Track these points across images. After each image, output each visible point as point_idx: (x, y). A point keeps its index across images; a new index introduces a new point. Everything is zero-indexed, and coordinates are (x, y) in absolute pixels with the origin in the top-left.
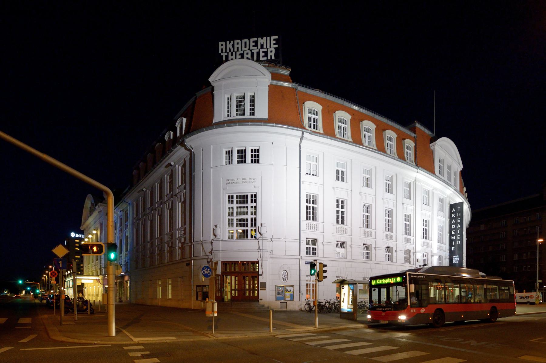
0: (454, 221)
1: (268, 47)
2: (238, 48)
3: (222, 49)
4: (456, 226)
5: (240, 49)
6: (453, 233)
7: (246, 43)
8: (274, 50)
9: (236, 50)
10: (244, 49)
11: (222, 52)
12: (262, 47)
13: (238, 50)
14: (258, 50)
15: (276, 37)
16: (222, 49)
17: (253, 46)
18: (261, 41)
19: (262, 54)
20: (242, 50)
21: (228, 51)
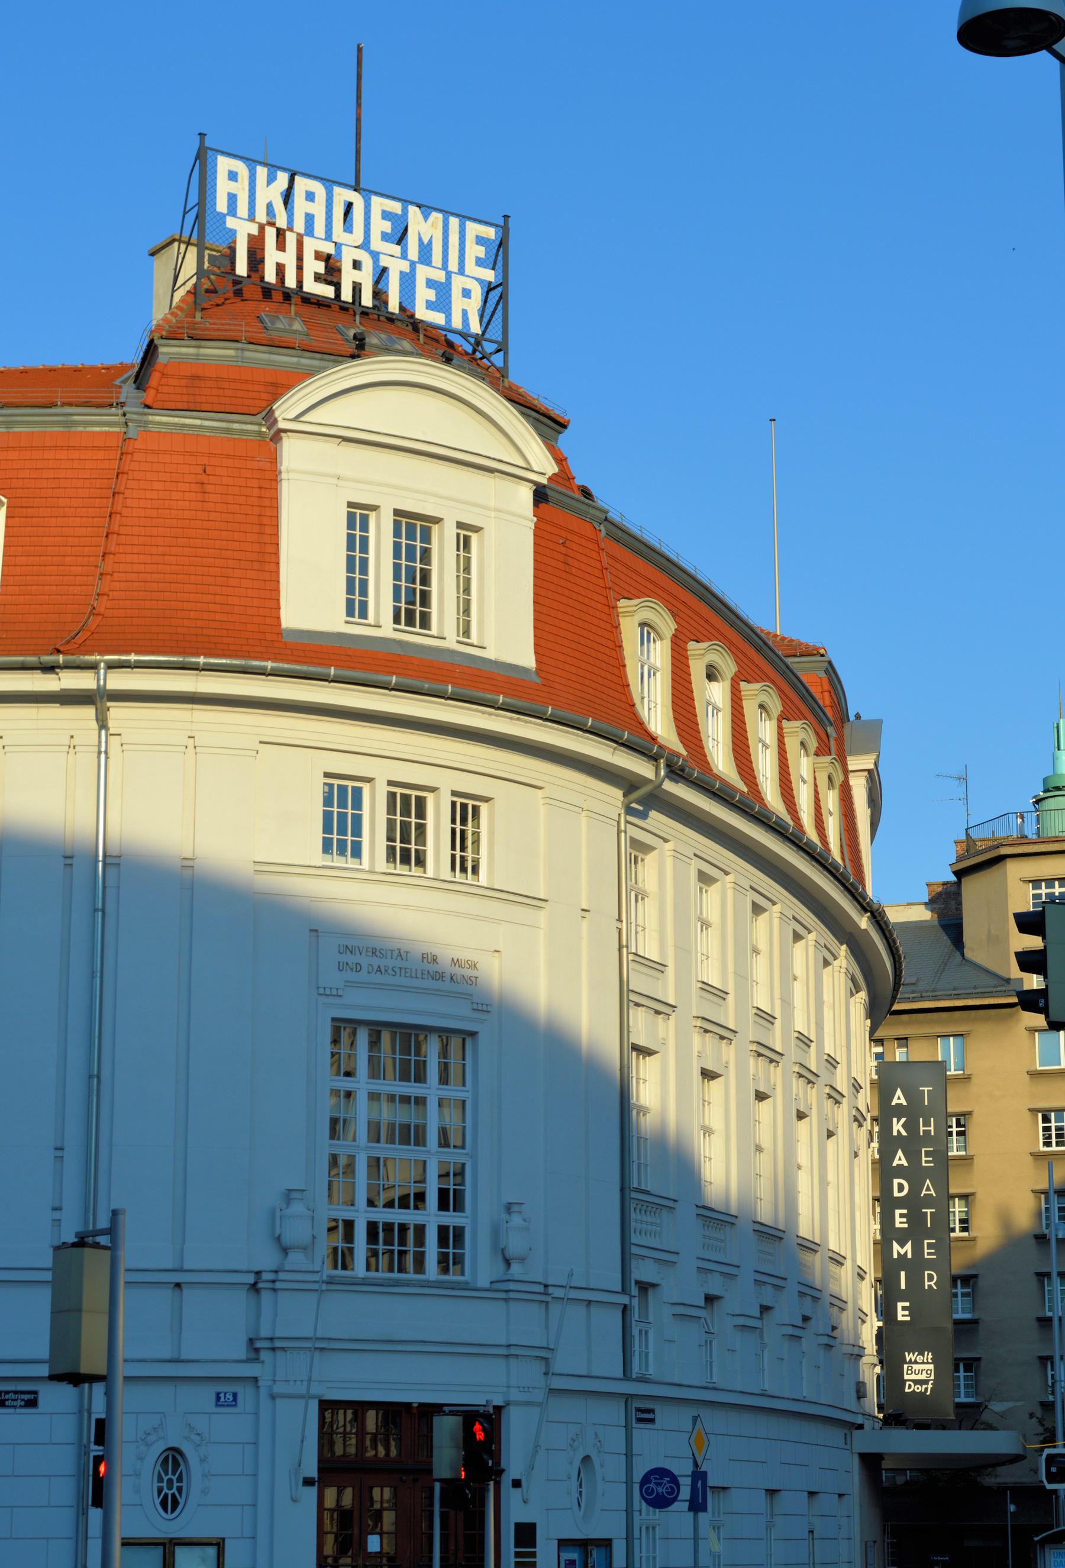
0: (900, 1159)
1: (453, 265)
2: (309, 219)
3: (232, 198)
4: (916, 1187)
5: (320, 228)
6: (900, 1222)
7: (349, 206)
8: (477, 293)
9: (299, 226)
12: (425, 250)
13: (310, 229)
14: (405, 266)
16: (232, 198)
17: (385, 237)
18: (423, 227)
19: (423, 294)
20: (328, 237)
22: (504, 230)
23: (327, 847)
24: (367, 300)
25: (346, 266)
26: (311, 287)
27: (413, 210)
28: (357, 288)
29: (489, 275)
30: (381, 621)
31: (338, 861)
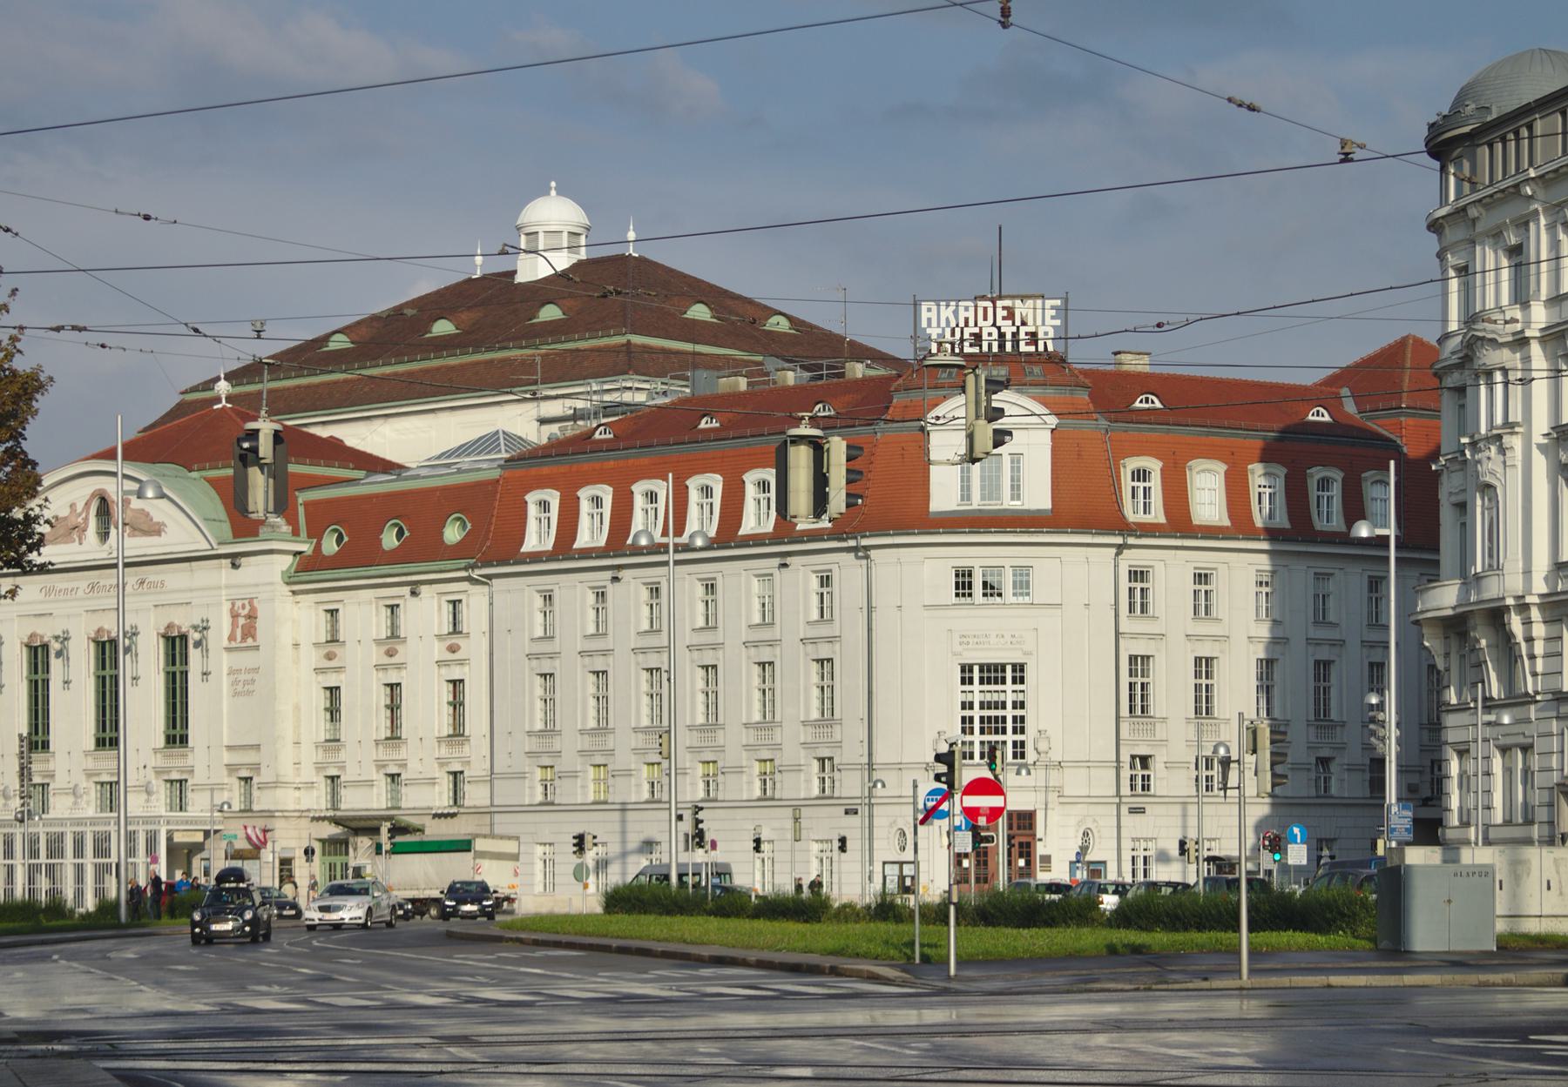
1: (1039, 322)
3: (929, 320)
5: (971, 323)
7: (985, 309)
9: (962, 324)
10: (981, 322)
11: (929, 325)
13: (967, 325)
15: (1058, 302)
16: (929, 320)
17: (1004, 318)
18: (1021, 309)
21: (943, 324)
22: (1066, 301)
23: (957, 595)
24: (995, 349)
25: (985, 336)
27: (1018, 302)
28: (990, 346)
29: (1058, 322)
30: (976, 503)
31: (963, 600)
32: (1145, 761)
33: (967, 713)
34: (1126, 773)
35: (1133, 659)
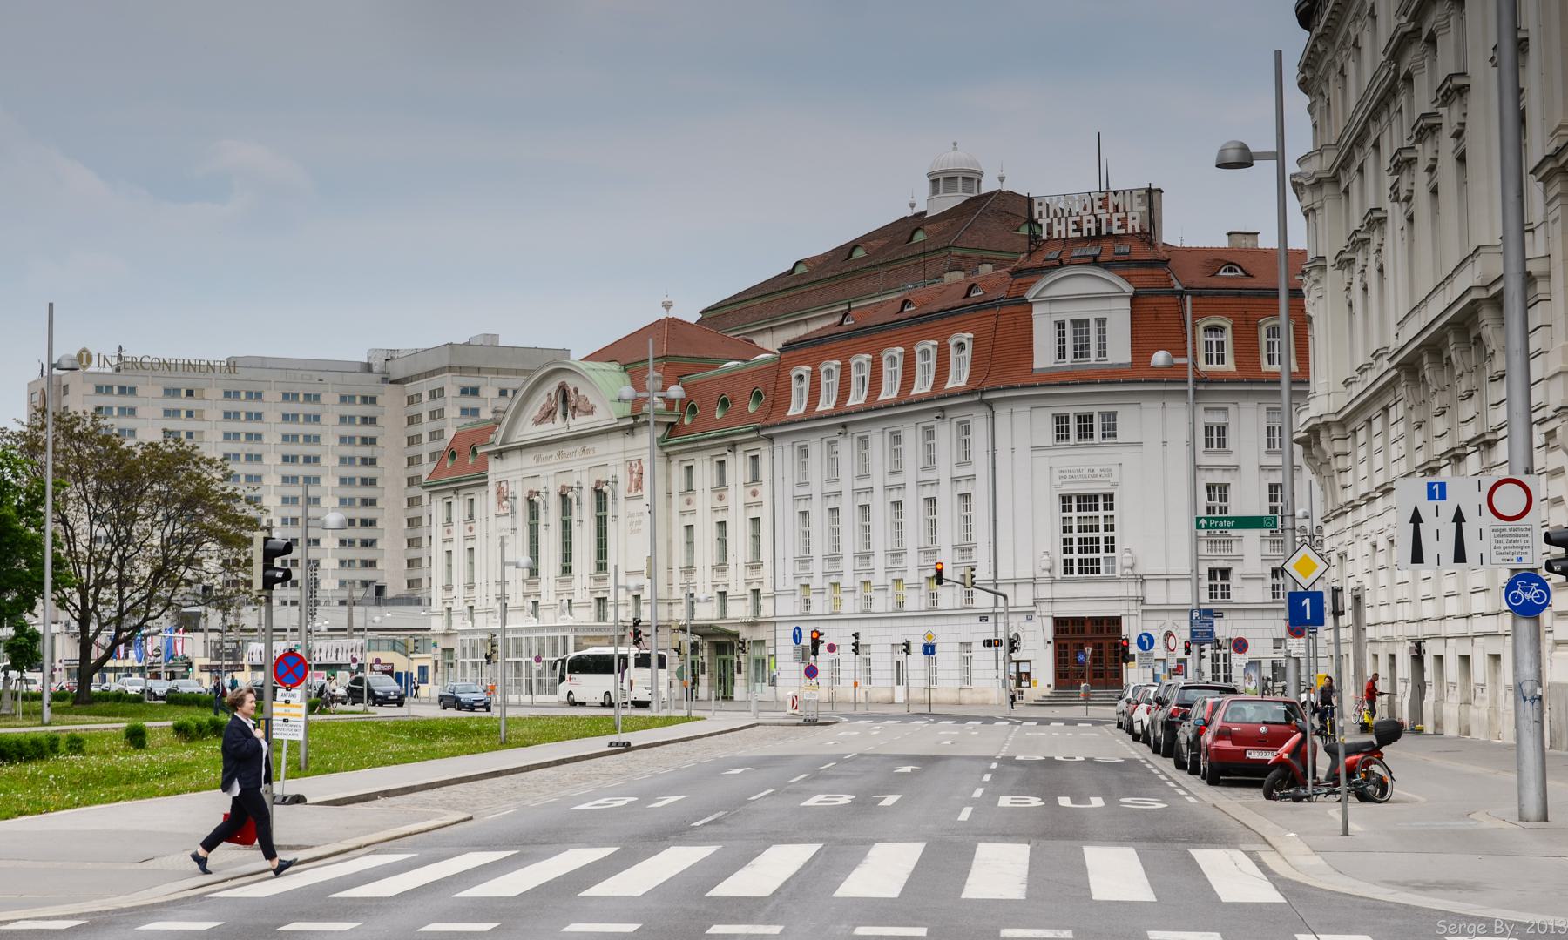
8: (1138, 216)
12: (1116, 209)
19: (1116, 224)
26: (1071, 235)
32: (1225, 573)
33: (1068, 535)
34: (1205, 583)
35: (1210, 487)
